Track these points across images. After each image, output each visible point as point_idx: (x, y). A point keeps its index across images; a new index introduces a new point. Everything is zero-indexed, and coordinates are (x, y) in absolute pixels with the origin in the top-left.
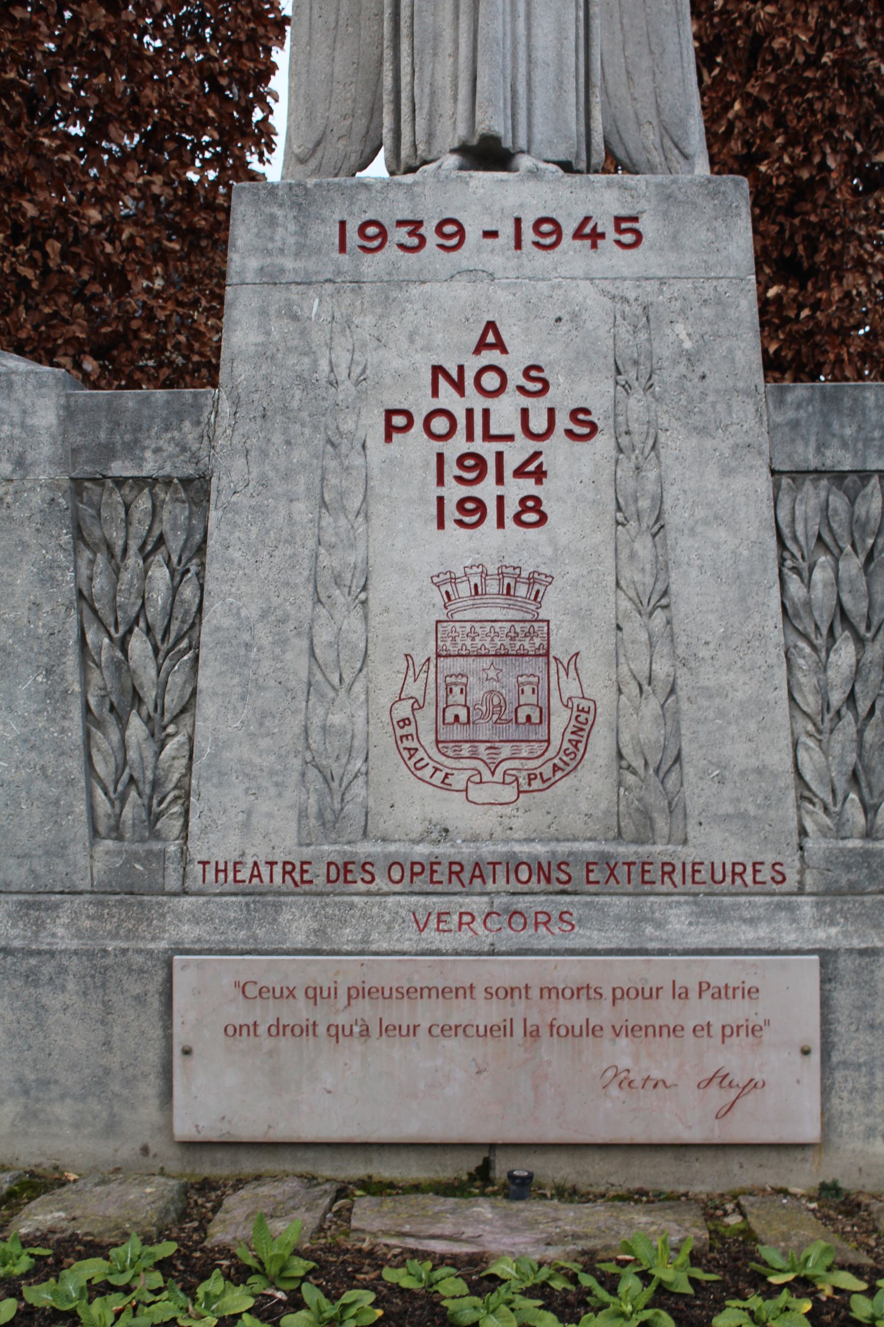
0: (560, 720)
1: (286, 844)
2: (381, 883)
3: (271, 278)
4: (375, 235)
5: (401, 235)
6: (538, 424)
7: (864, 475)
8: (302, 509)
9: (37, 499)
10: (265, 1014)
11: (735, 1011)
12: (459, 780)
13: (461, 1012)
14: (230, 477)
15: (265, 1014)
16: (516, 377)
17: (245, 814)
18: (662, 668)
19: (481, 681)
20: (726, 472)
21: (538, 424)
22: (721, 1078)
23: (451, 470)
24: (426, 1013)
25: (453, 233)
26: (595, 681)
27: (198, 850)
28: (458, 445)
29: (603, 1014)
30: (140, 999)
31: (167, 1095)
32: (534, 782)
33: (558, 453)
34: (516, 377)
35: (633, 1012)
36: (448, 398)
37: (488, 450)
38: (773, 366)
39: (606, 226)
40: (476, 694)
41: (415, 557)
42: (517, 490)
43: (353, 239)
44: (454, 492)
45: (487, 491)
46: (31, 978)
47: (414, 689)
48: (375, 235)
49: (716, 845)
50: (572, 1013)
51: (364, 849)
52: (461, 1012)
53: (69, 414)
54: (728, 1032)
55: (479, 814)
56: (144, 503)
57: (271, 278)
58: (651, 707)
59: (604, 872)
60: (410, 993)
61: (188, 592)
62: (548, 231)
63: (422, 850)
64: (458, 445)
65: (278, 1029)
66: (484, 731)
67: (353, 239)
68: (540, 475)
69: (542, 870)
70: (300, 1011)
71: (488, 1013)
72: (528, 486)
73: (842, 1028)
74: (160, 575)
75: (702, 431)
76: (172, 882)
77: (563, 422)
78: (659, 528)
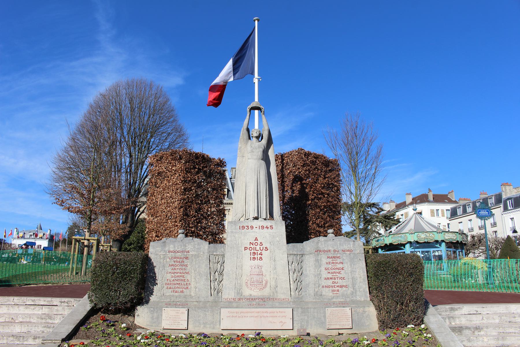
0: (264, 282)
1: (233, 297)
2: (244, 301)
3: (232, 232)
4: (243, 227)
5: (246, 228)
6: (262, 249)
7: (297, 255)
8: (235, 258)
9: (205, 257)
10: (231, 315)
11: (283, 314)
12: (253, 289)
13: (253, 314)
14: (227, 255)
15: (231, 315)
16: (259, 244)
17: (228, 293)
18: (275, 276)
19: (255, 278)
20: (282, 254)
21: (262, 249)
22: (281, 322)
23: (252, 254)
24: (249, 315)
25: (252, 227)
26: (268, 278)
27: (223, 297)
28: (253, 251)
29: (268, 315)
30: (217, 313)
31: (220, 324)
32: (261, 289)
33: (264, 252)
34: (259, 244)
35: (272, 314)
36: (251, 246)
37: (256, 252)
38: (289, 241)
39: (269, 227)
40: (255, 279)
41: (248, 264)
42: (259, 256)
43: (241, 228)
44: (252, 256)
45: (256, 256)
46: (205, 311)
47: (248, 279)
48: (243, 227)
49: (281, 296)
50: (265, 315)
51: (242, 297)
52: (253, 314)
53: (209, 247)
54: (282, 317)
55: (255, 293)
56: (217, 257)
57: (232, 232)
58: (274, 281)
59: (269, 299)
60: (247, 312)
61: (222, 267)
62: (263, 227)
63: (248, 297)
64: (253, 251)
65: (233, 316)
66: (255, 283)
67: (241, 228)
68: (262, 255)
69: (262, 299)
70: (235, 315)
71: (256, 315)
72: (260, 256)
73: (294, 316)
74: (219, 265)
75: (280, 250)
76: (220, 301)
77: (264, 249)
78: (275, 261)
